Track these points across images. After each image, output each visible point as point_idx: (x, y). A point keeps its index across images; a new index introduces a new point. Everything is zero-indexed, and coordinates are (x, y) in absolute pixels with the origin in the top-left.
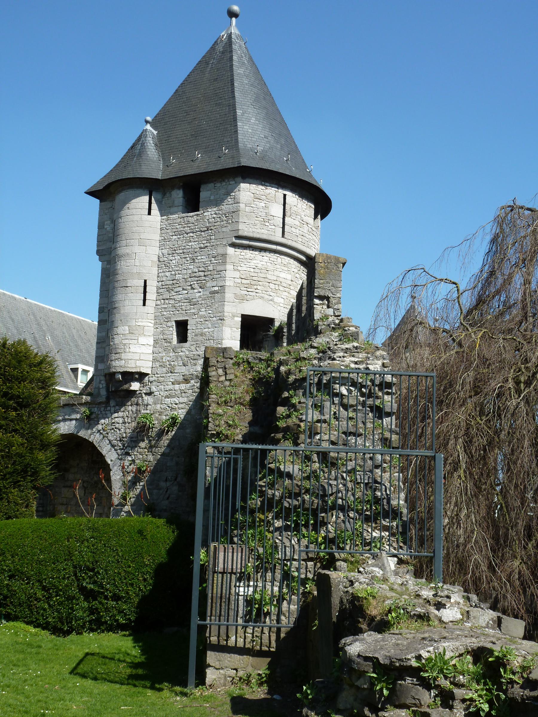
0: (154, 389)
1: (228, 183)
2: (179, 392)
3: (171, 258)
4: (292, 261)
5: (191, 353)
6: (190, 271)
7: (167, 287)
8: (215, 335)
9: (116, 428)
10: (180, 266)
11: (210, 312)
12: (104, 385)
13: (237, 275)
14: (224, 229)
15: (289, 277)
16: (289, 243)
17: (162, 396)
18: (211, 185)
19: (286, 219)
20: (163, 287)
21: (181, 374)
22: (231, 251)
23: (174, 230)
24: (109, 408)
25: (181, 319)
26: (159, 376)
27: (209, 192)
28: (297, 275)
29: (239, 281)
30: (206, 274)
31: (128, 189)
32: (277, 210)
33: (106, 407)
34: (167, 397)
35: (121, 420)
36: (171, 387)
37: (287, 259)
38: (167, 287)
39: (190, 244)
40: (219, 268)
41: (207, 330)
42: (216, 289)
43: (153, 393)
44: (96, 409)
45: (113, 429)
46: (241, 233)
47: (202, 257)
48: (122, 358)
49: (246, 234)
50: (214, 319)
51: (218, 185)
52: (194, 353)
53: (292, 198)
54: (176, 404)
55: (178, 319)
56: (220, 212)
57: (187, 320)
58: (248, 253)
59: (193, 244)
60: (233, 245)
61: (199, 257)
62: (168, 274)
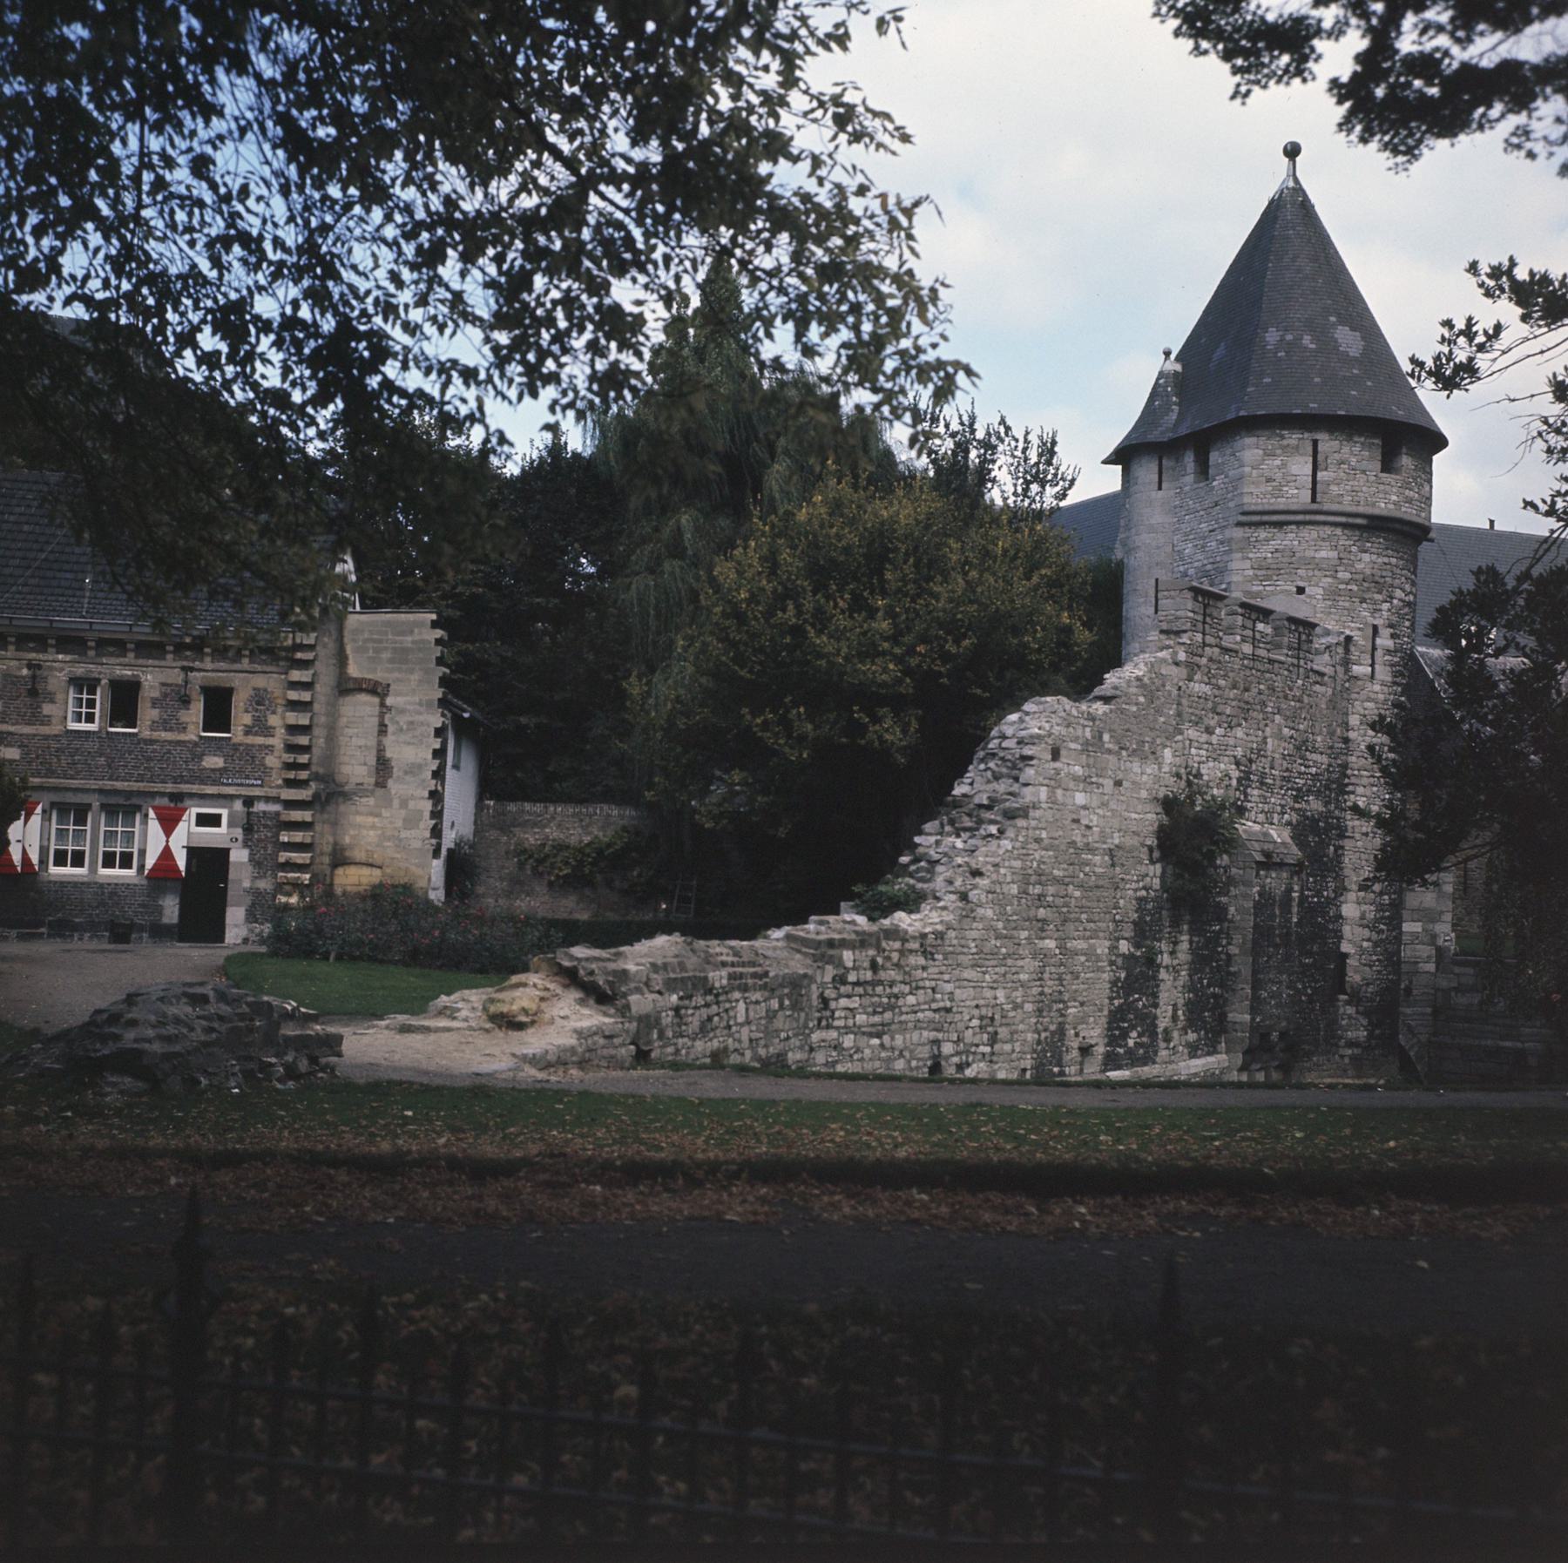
4: (1339, 531)
13: (1248, 564)
15: (1333, 554)
16: (1326, 507)
19: (1319, 475)
22: (1239, 533)
28: (1354, 549)
29: (1251, 572)
32: (1301, 467)
37: (1328, 530)
40: (1226, 558)
46: (1246, 508)
49: (1253, 508)
53: (1328, 444)
58: (1263, 534)
60: (1240, 524)
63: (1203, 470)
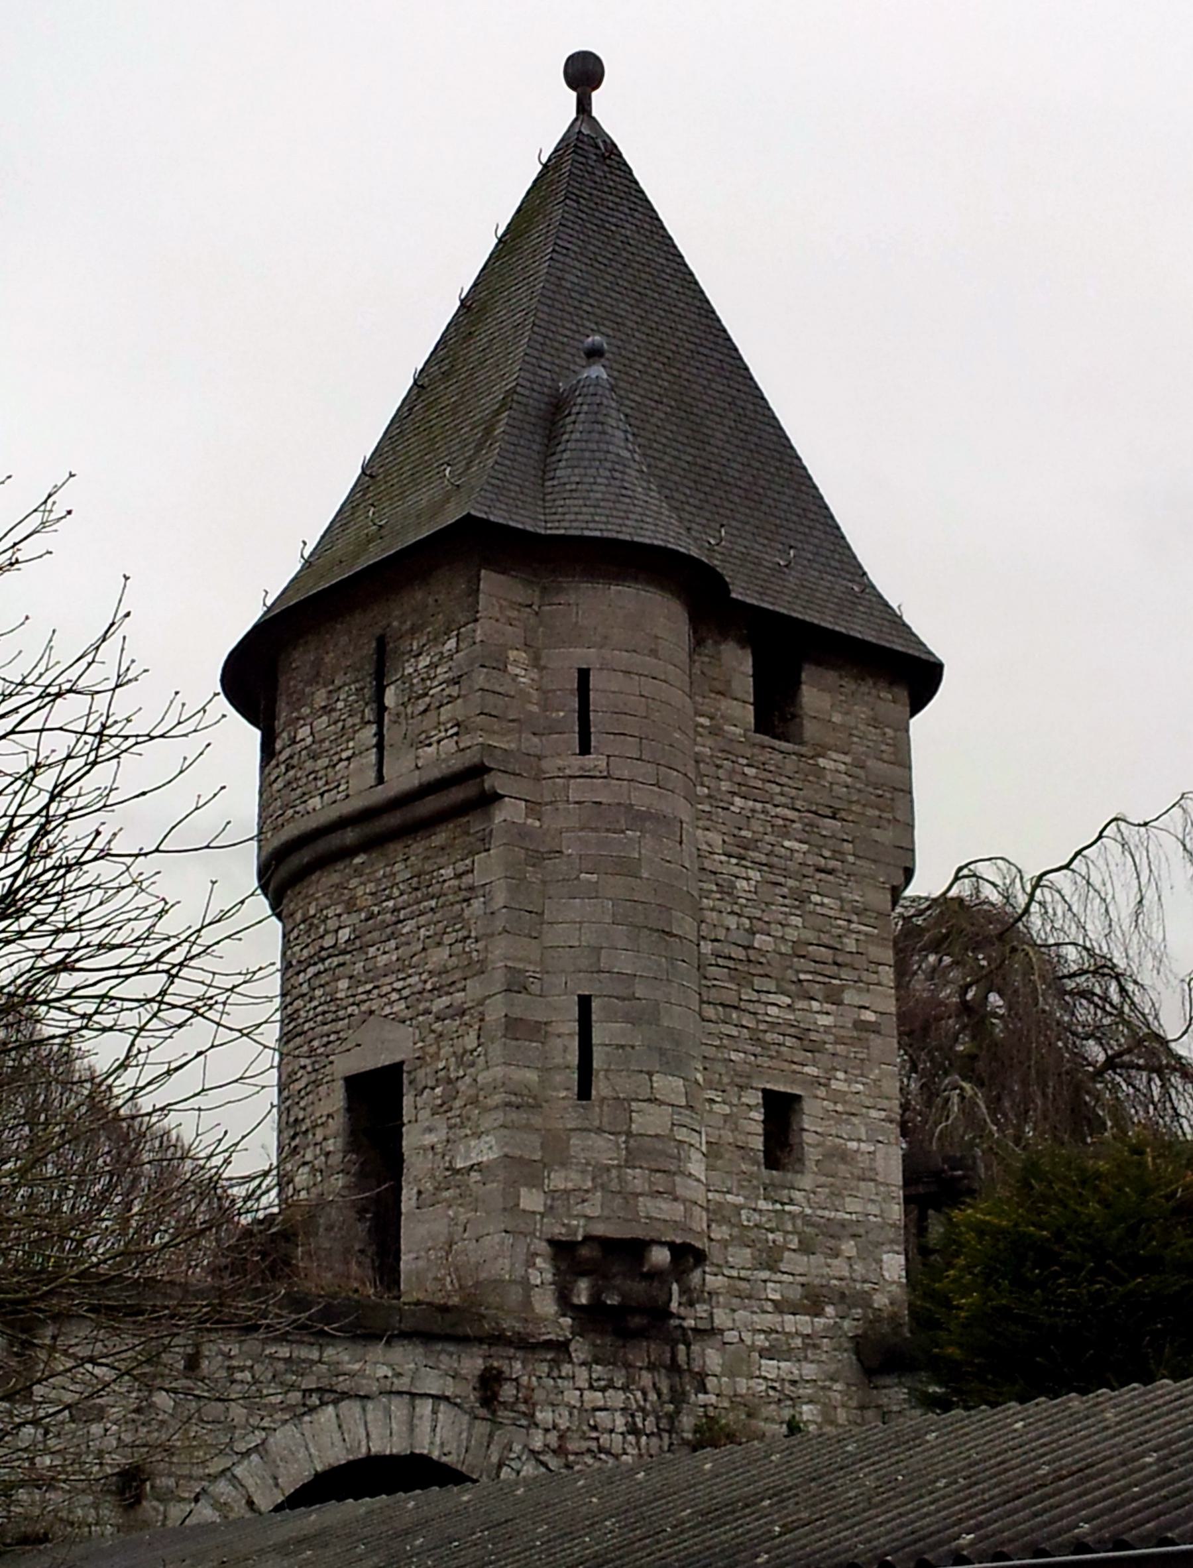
0: (721, 1318)
1: (874, 692)
2: (798, 1342)
3: (736, 870)
5: (819, 1212)
6: (792, 934)
7: (731, 964)
8: (880, 1169)
9: (601, 1450)
10: (763, 906)
11: (861, 1087)
12: (549, 1277)
14: (876, 834)
17: (752, 1348)
18: (831, 676)
20: (721, 961)
21: (799, 1279)
23: (738, 779)
24: (566, 1369)
25: (782, 1089)
26: (734, 1273)
27: (827, 697)
30: (840, 960)
31: (649, 582)
33: (555, 1363)
34: (765, 1353)
35: (620, 1422)
36: (771, 1320)
38: (731, 964)
39: (787, 844)
41: (853, 1145)
42: (869, 1016)
43: (721, 1331)
44: (518, 1365)
45: (589, 1450)
47: (826, 900)
48: (679, 1191)
50: (874, 1113)
51: (850, 685)
52: (826, 1213)
54: (794, 1383)
55: (768, 1086)
56: (859, 772)
57: (798, 1098)
59: (796, 845)
61: (816, 898)
62: (732, 922)
63: (776, 712)
